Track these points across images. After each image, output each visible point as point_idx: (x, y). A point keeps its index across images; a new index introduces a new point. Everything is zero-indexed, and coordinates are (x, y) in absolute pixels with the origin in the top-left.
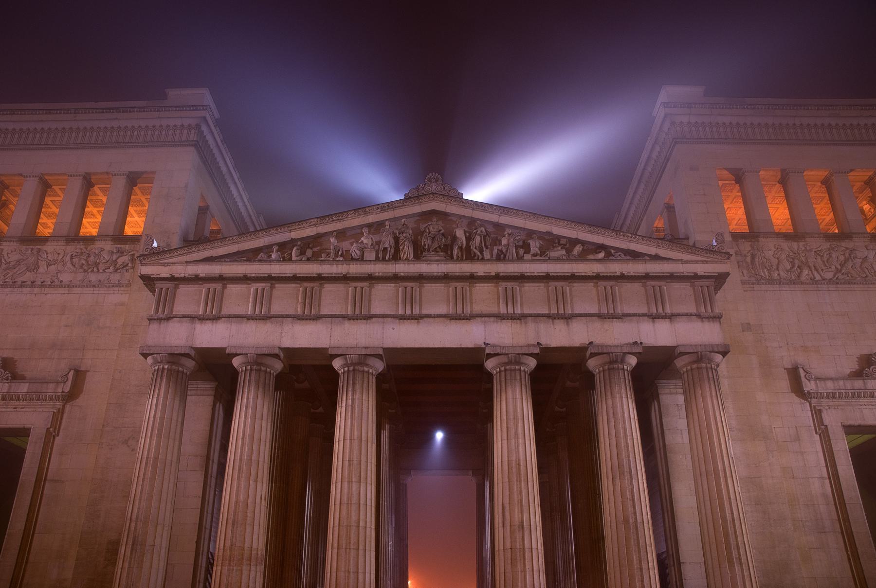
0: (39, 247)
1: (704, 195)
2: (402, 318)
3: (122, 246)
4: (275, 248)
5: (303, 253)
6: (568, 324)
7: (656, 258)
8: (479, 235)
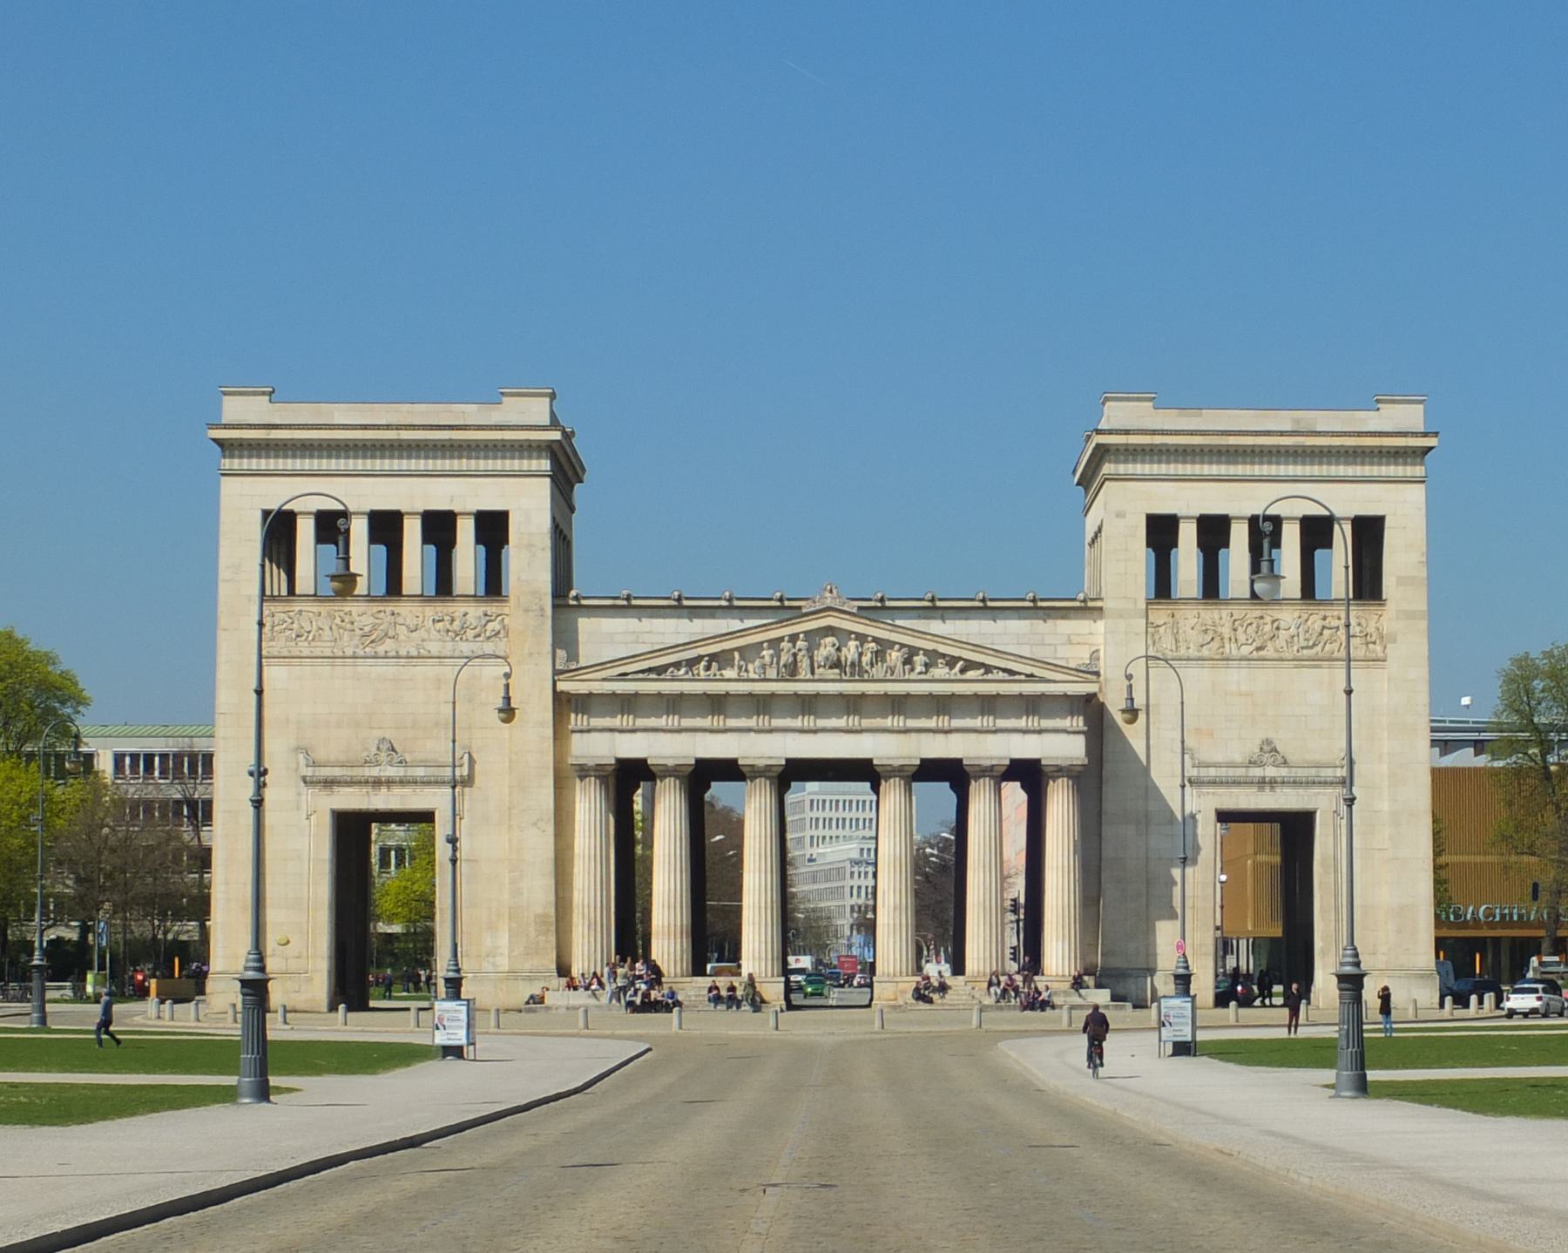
0: (390, 608)
3: (488, 608)
5: (708, 668)
7: (1032, 675)
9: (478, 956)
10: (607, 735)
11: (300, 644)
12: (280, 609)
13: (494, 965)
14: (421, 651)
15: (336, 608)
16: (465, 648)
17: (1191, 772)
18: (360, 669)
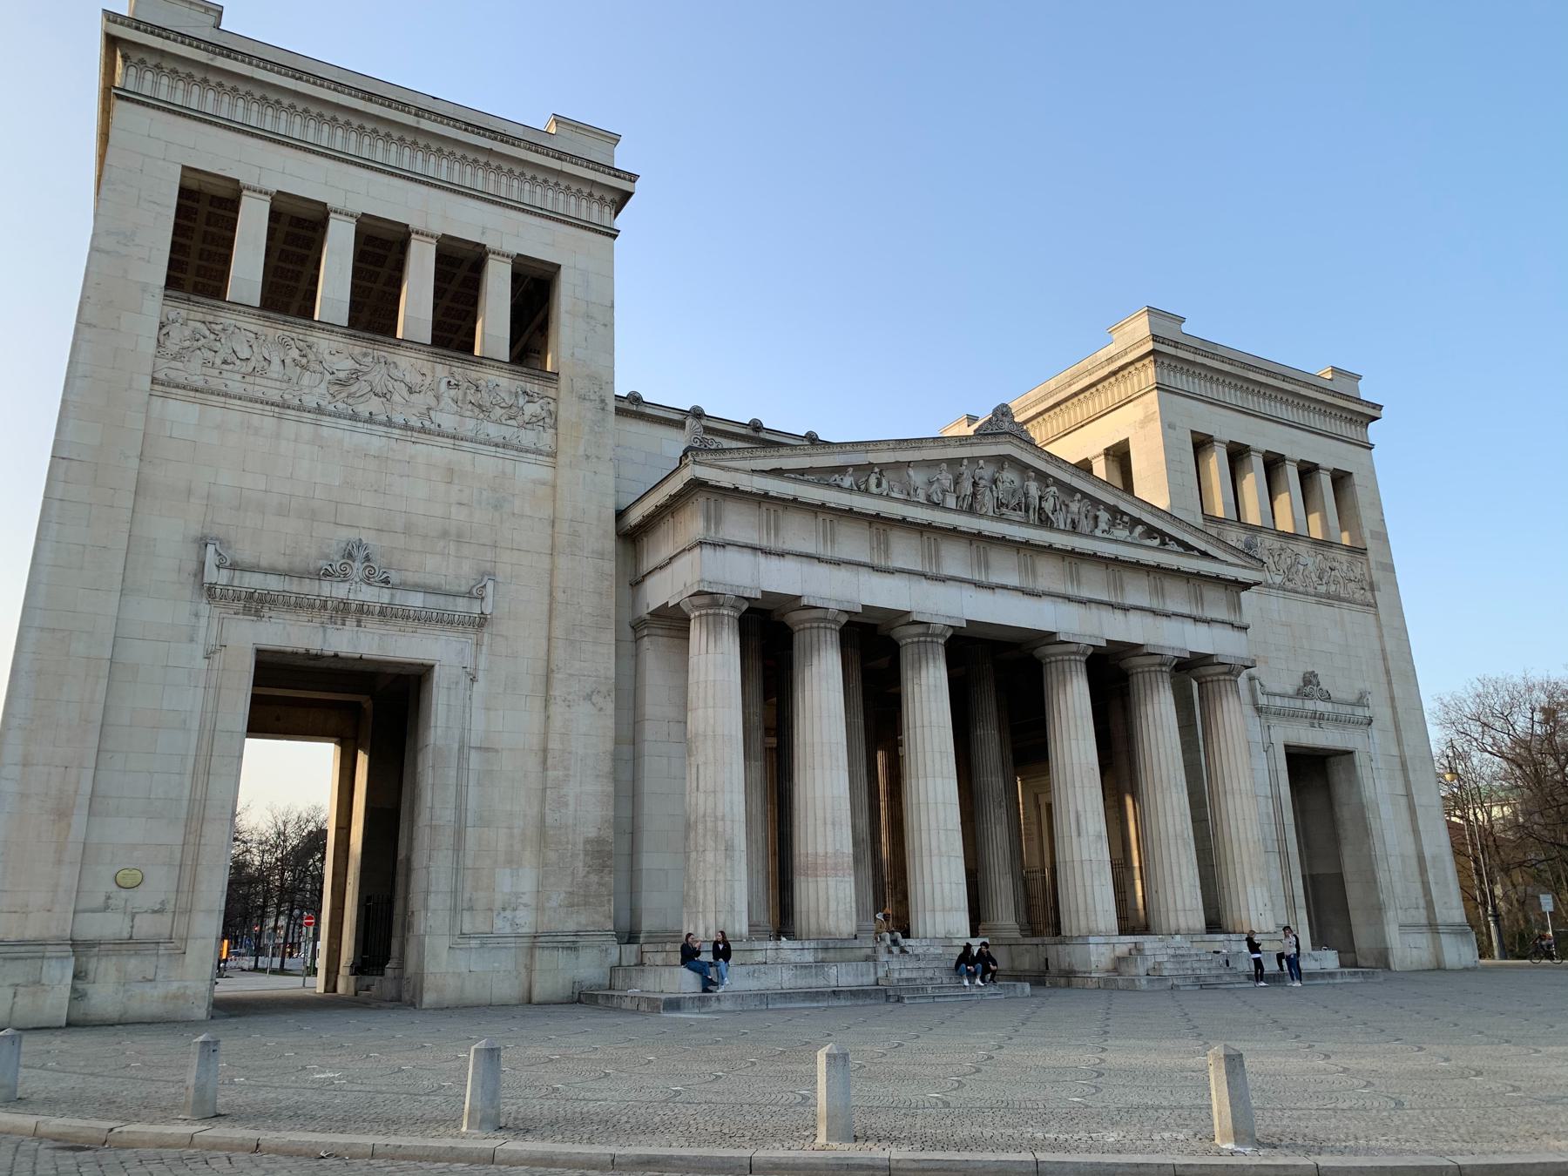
1: (1180, 462)
2: (978, 585)
4: (851, 469)
5: (879, 485)
6: (1126, 614)
7: (1204, 554)
8: (1052, 496)
9: (491, 910)
10: (746, 558)
11: (224, 373)
12: (200, 316)
13: (514, 924)
14: (427, 423)
15: (294, 335)
16: (494, 431)
17: (1263, 700)
18: (325, 432)
